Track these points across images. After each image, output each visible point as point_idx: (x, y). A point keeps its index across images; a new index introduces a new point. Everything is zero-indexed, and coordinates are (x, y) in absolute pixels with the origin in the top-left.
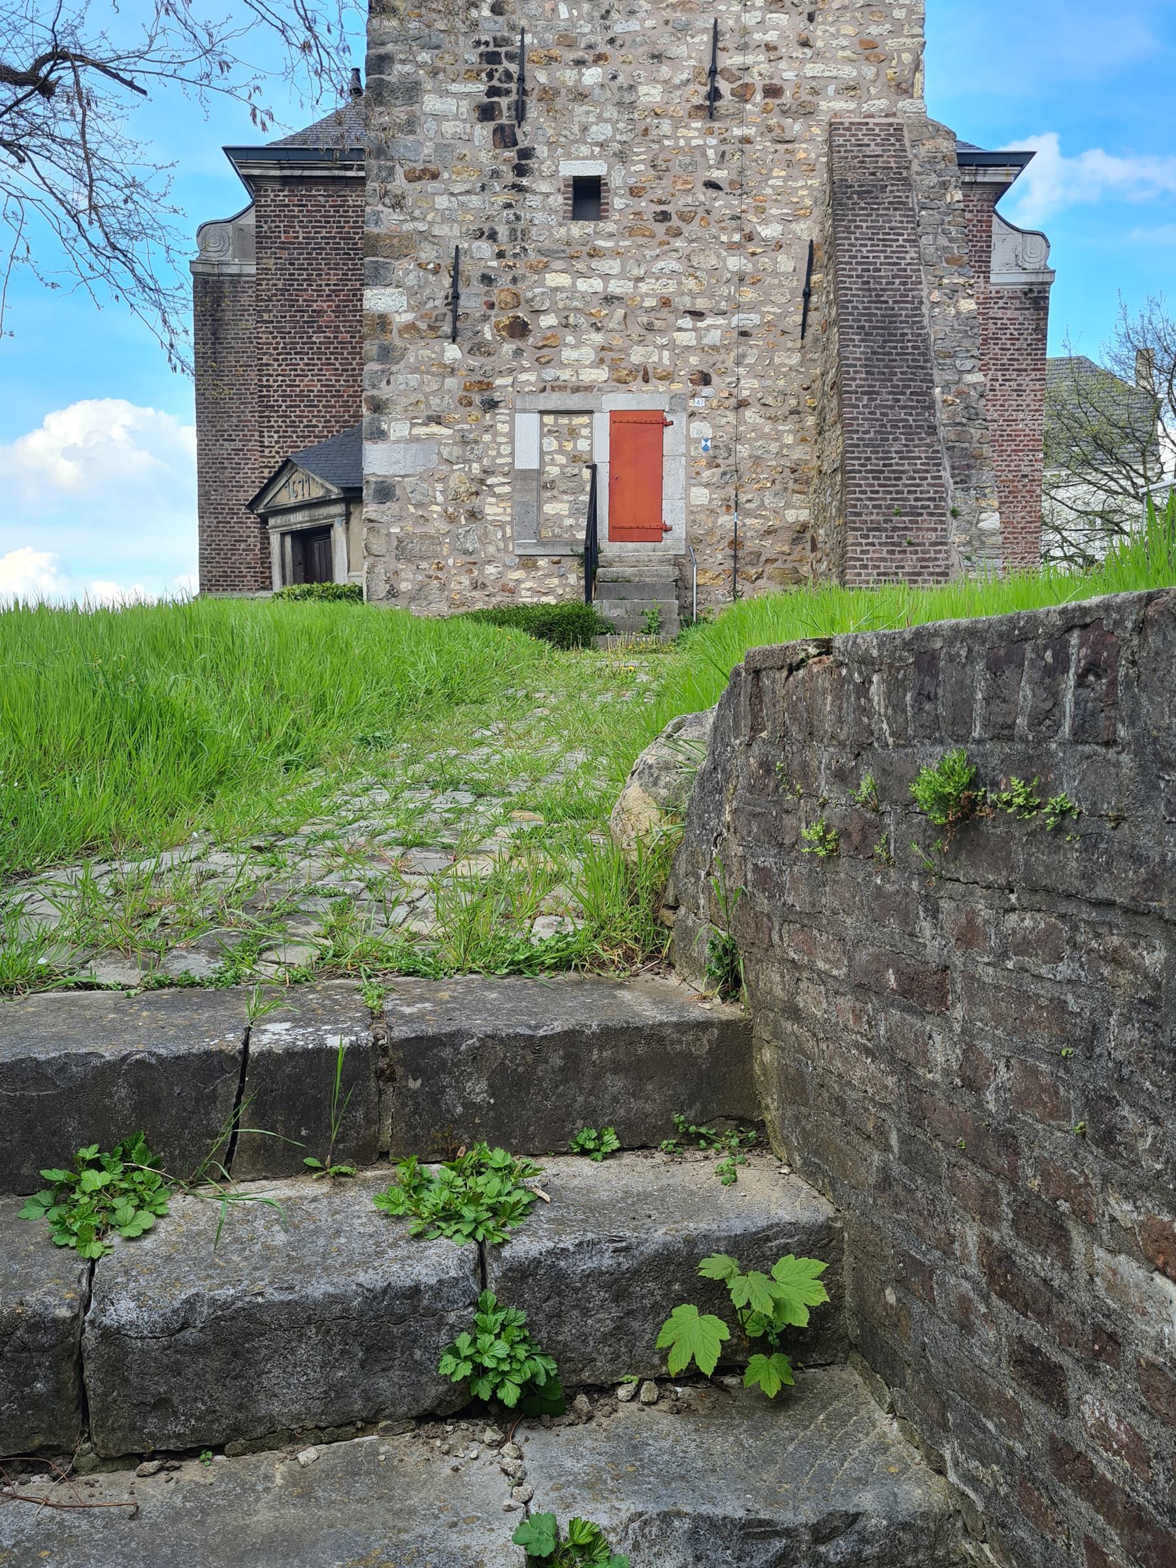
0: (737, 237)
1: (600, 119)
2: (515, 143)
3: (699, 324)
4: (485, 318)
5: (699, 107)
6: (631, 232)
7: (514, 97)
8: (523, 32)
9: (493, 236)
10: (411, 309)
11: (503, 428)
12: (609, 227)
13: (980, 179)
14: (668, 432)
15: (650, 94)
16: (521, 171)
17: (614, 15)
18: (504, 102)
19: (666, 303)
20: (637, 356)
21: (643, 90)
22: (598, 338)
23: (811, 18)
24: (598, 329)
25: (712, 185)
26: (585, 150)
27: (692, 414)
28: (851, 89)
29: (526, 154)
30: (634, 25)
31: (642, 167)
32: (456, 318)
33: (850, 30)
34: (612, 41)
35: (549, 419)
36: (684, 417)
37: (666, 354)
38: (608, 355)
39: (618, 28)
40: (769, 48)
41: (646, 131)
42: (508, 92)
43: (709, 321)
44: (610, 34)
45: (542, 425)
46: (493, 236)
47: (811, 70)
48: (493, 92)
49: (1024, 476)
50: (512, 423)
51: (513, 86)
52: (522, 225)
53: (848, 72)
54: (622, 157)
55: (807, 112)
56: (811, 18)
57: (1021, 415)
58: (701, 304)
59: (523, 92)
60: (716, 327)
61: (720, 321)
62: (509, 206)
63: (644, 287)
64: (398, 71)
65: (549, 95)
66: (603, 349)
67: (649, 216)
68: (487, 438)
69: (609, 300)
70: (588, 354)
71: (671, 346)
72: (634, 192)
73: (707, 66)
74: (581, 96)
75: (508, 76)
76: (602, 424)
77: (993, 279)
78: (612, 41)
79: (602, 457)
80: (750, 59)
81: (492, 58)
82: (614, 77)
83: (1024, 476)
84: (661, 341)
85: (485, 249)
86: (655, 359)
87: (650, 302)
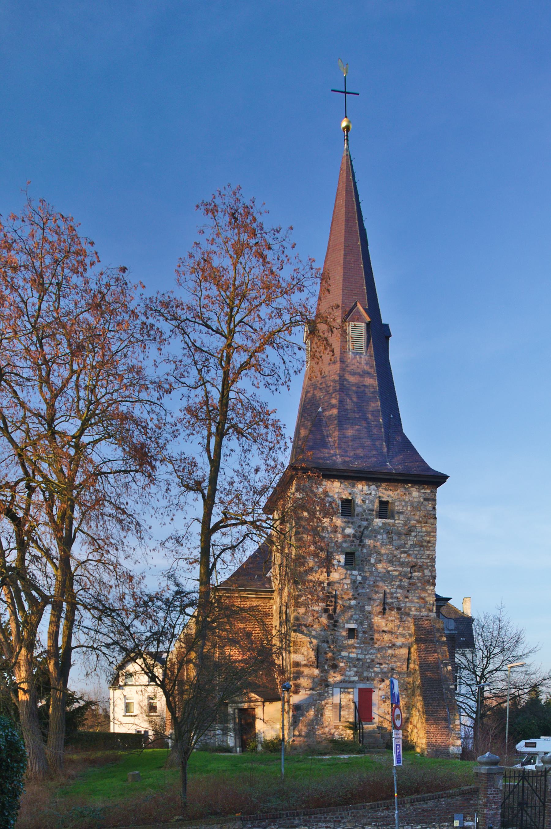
0: (390, 645)
1: (355, 614)
2: (333, 619)
3: (382, 667)
4: (325, 664)
5: (381, 612)
6: (364, 643)
7: (333, 607)
8: (336, 591)
9: (328, 642)
11: (331, 692)
14: (373, 694)
16: (335, 626)
17: (359, 588)
18: (330, 608)
20: (365, 674)
21: (366, 607)
22: (355, 669)
23: (408, 591)
24: (355, 667)
26: (352, 621)
27: (380, 689)
30: (364, 591)
31: (366, 626)
32: (318, 663)
34: (358, 594)
35: (342, 690)
36: (378, 690)
37: (373, 674)
38: (358, 674)
39: (360, 591)
41: (367, 617)
42: (331, 606)
43: (384, 666)
44: (358, 593)
45: (341, 691)
46: (328, 642)
50: (333, 690)
51: (333, 604)
52: (335, 640)
54: (361, 623)
56: (408, 591)
58: (381, 661)
60: (385, 667)
61: (386, 666)
62: (331, 635)
63: (367, 657)
68: (326, 694)
69: (358, 660)
70: (352, 673)
71: (374, 672)
72: (364, 632)
73: (383, 602)
75: (332, 602)
78: (358, 594)
80: (393, 600)
82: (359, 603)
84: (372, 670)
85: (325, 645)
86: (370, 675)
87: (369, 661)
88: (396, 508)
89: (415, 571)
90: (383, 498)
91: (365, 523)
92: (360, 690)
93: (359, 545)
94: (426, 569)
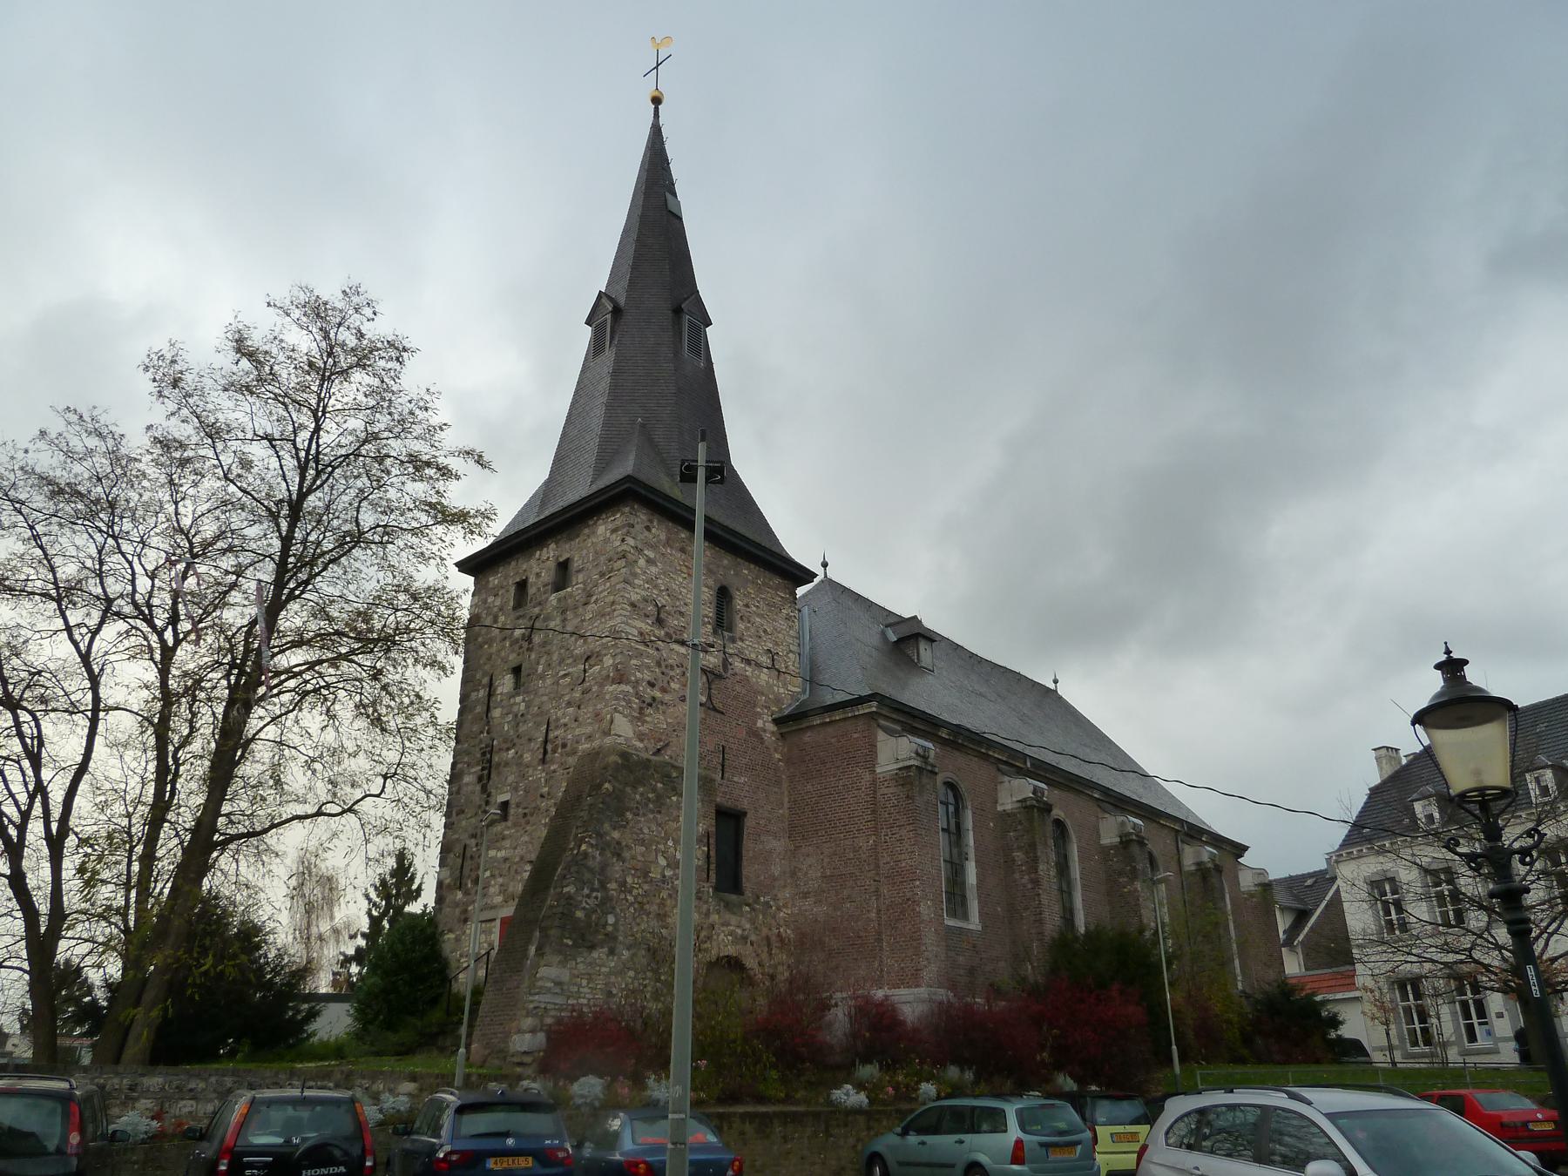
10: (451, 875)
12: (509, 823)
13: (857, 713)
15: (527, 757)
19: (522, 858)
22: (500, 880)
23: (579, 708)
25: (542, 796)
28: (590, 737)
29: (489, 796)
33: (591, 709)
40: (565, 725)
47: (577, 732)
48: (483, 769)
49: (908, 900)
53: (589, 730)
54: (516, 789)
55: (574, 752)
56: (579, 708)
57: (903, 857)
59: (490, 767)
64: (459, 766)
65: (499, 764)
66: (501, 885)
67: (521, 816)
74: (507, 764)
76: (498, 922)
77: (878, 770)
79: (496, 944)
81: (484, 754)
83: (908, 900)
85: (473, 842)
88: (576, 565)
89: (591, 666)
90: (561, 556)
91: (537, 610)
92: (504, 921)
93: (528, 649)
94: (605, 655)
